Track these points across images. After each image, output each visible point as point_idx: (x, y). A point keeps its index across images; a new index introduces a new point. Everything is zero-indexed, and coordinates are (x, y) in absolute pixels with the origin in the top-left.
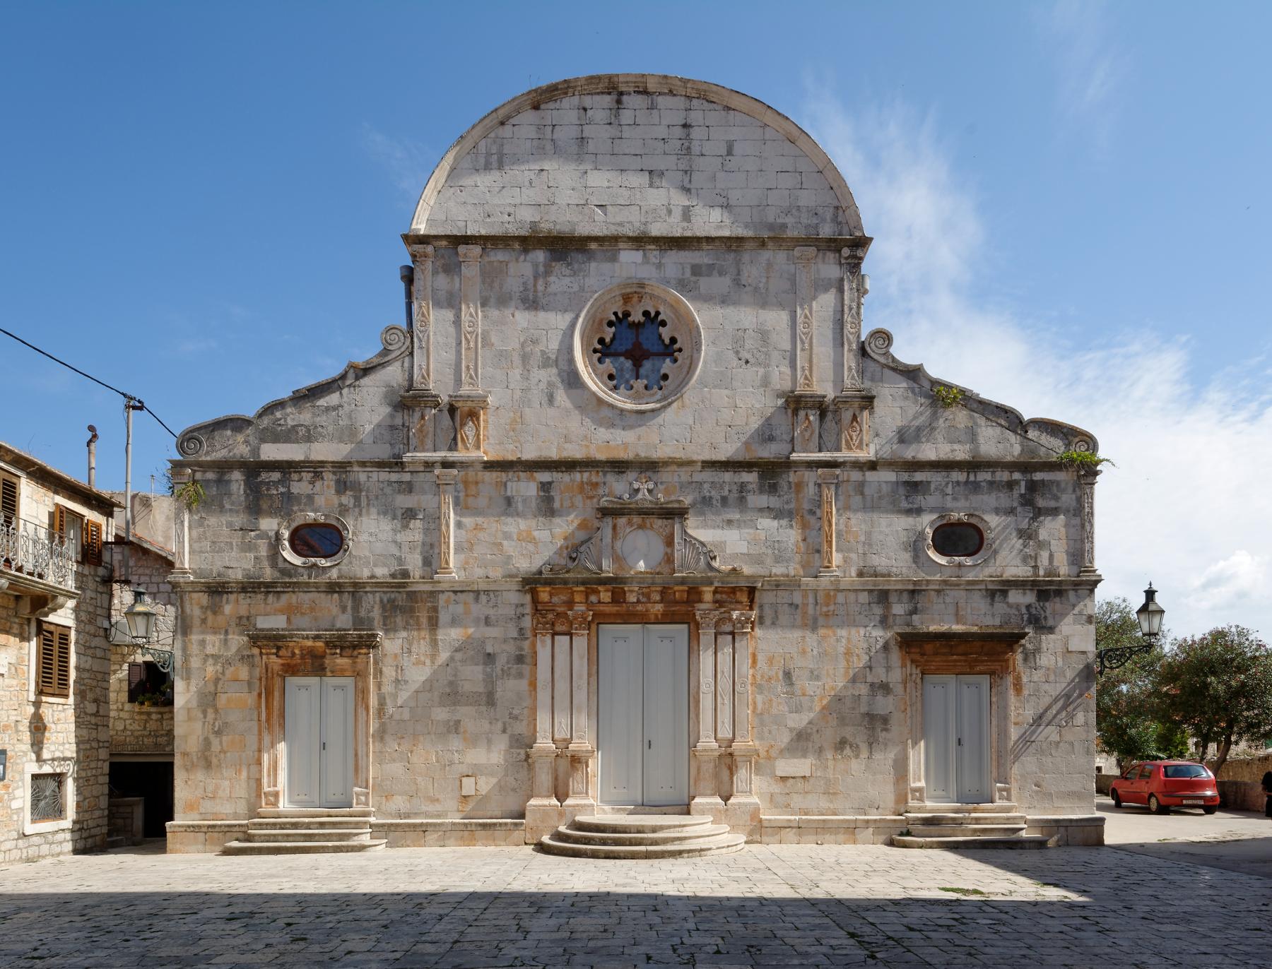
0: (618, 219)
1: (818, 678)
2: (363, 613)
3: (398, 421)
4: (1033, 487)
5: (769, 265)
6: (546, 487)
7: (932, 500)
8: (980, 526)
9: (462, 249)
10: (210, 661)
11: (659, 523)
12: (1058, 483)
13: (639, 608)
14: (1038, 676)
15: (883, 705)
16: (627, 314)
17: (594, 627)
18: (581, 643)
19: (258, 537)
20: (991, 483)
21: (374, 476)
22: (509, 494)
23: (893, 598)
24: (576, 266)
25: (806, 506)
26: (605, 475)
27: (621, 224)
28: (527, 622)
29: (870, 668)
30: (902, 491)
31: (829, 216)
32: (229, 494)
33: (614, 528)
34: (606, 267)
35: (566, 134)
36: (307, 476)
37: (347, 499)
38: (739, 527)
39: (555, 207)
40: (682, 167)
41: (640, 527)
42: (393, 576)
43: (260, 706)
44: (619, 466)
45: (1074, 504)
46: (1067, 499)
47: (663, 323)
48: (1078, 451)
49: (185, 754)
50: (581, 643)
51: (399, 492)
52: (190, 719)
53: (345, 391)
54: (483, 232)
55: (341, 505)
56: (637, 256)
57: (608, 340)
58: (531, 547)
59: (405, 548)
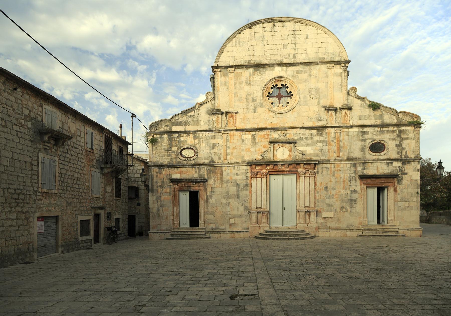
0: (274, 59)
1: (335, 189)
2: (201, 173)
3: (211, 119)
4: (400, 132)
6: (254, 136)
8: (384, 143)
9: (229, 69)
10: (159, 187)
11: (287, 145)
12: (408, 130)
14: (402, 187)
15: (355, 196)
16: (277, 85)
17: (268, 175)
18: (264, 180)
19: (172, 153)
20: (388, 131)
21: (204, 134)
22: (243, 138)
23: (358, 165)
24: (262, 72)
25: (331, 139)
27: (275, 60)
28: (249, 175)
29: (351, 186)
30: (360, 134)
31: (337, 55)
32: (163, 141)
33: (274, 147)
34: (271, 72)
35: (258, 35)
36: (185, 135)
37: (196, 141)
39: (255, 56)
42: (210, 162)
43: (173, 199)
44: (275, 129)
46: (411, 135)
47: (287, 87)
48: (415, 120)
49: (152, 213)
50: (264, 180)
52: (153, 203)
53: (196, 111)
54: (235, 64)
55: (195, 143)
56: (280, 69)
58: (249, 153)
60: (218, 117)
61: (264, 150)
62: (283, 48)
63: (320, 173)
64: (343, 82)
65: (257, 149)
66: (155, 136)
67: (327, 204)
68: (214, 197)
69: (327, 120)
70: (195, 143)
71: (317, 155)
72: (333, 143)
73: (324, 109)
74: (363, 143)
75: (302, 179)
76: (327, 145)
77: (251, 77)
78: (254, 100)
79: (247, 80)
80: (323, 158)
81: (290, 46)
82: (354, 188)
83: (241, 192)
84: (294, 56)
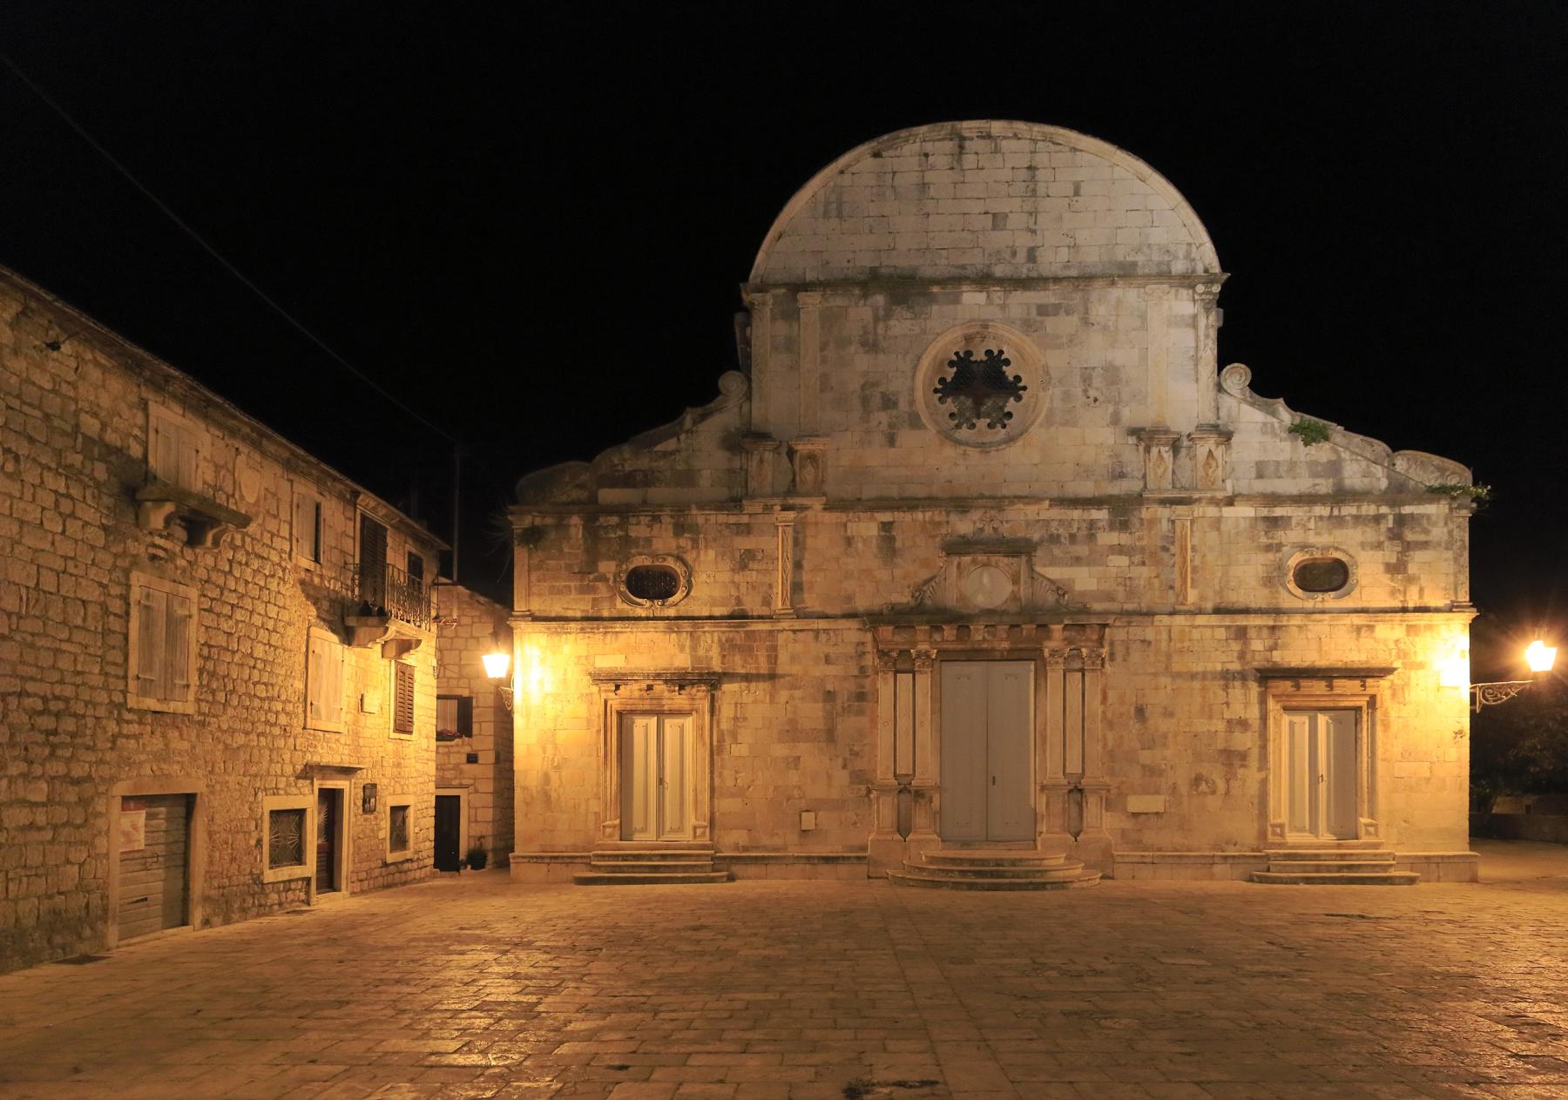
0: (962, 262)
1: (1172, 715)
3: (736, 464)
4: (1401, 520)
5: (1119, 302)
6: (886, 527)
7: (1291, 536)
9: (801, 296)
11: (1005, 561)
12: (1428, 517)
13: (985, 646)
15: (1245, 741)
16: (969, 353)
17: (937, 665)
18: (924, 681)
20: (1357, 518)
23: (1252, 633)
24: (917, 309)
26: (948, 514)
27: (963, 267)
28: (870, 660)
29: (1228, 704)
30: (1261, 526)
31: (1181, 254)
34: (949, 308)
35: (908, 180)
36: (644, 520)
37: (685, 542)
38: (1088, 565)
40: (1026, 208)
41: (984, 565)
45: (1446, 537)
47: (1007, 362)
49: (525, 788)
50: (924, 681)
51: (737, 534)
53: (683, 437)
55: (679, 547)
57: (949, 380)
59: (743, 589)
60: (761, 461)
61: (924, 574)
62: (995, 228)
63: (1119, 658)
64: (1201, 345)
65: (897, 572)
66: (538, 521)
67: (1144, 767)
68: (746, 736)
69: (1144, 476)
70: (679, 547)
71: (1110, 597)
73: (1132, 440)
74: (1270, 556)
75: (1054, 675)
76: (1143, 563)
77: (881, 326)
78: (889, 403)
79: (866, 333)
80: (1129, 607)
81: (1017, 221)
82: (1237, 711)
83: (839, 719)
84: (1032, 256)
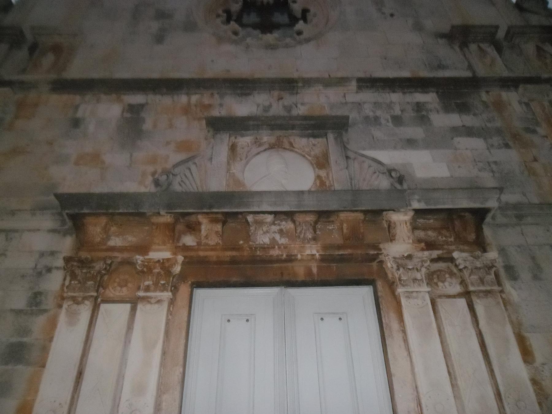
11: (301, 142)
13: (275, 253)
17: (184, 289)
22: (79, 114)
33: (233, 148)
41: (272, 147)
72: (536, 139)
73: (442, 41)
75: (415, 304)
